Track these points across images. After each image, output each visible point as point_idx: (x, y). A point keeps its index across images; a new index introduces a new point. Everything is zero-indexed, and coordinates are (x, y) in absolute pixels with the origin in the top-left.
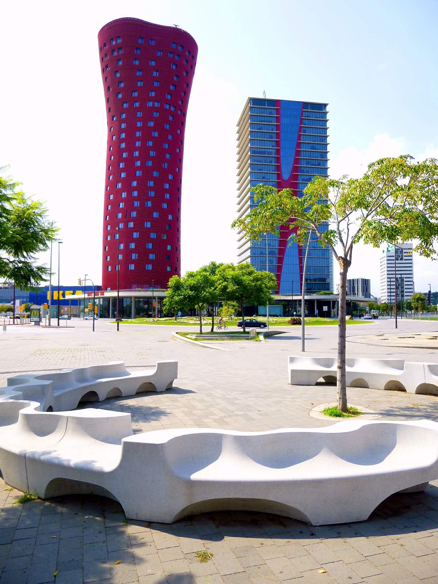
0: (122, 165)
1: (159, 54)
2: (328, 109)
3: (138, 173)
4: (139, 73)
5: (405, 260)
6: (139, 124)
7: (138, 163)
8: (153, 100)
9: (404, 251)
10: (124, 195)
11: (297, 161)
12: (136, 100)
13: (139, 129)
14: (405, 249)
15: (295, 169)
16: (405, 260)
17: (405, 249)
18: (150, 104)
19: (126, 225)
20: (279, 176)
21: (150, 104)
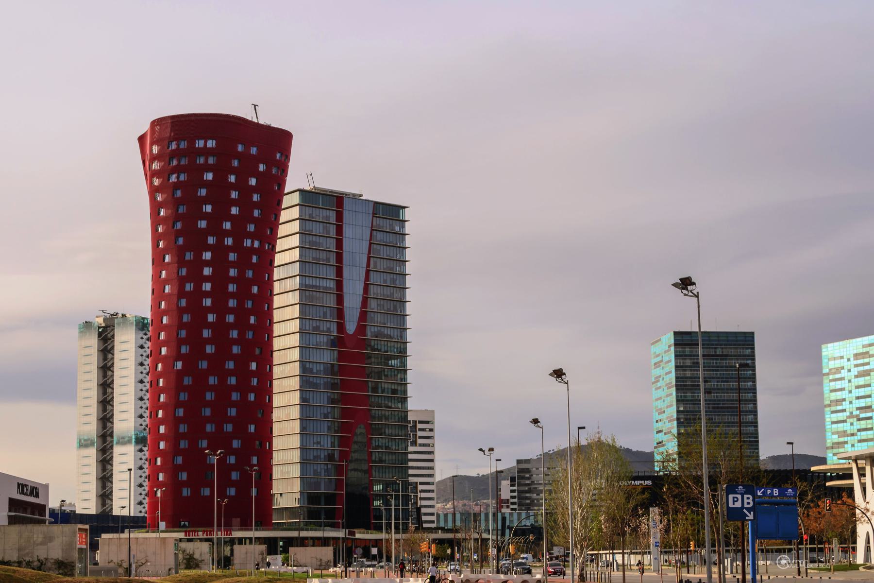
0: (206, 333)
1: (262, 168)
2: (407, 214)
3: (236, 350)
4: (234, 195)
5: (420, 445)
6: (233, 272)
7: (234, 334)
8: (252, 236)
9: (419, 426)
10: (212, 380)
11: (365, 302)
12: (227, 233)
13: (233, 280)
14: (421, 422)
15: (363, 316)
16: (420, 445)
17: (421, 422)
18: (248, 243)
19: (219, 428)
20: (341, 327)
21: (248, 243)
